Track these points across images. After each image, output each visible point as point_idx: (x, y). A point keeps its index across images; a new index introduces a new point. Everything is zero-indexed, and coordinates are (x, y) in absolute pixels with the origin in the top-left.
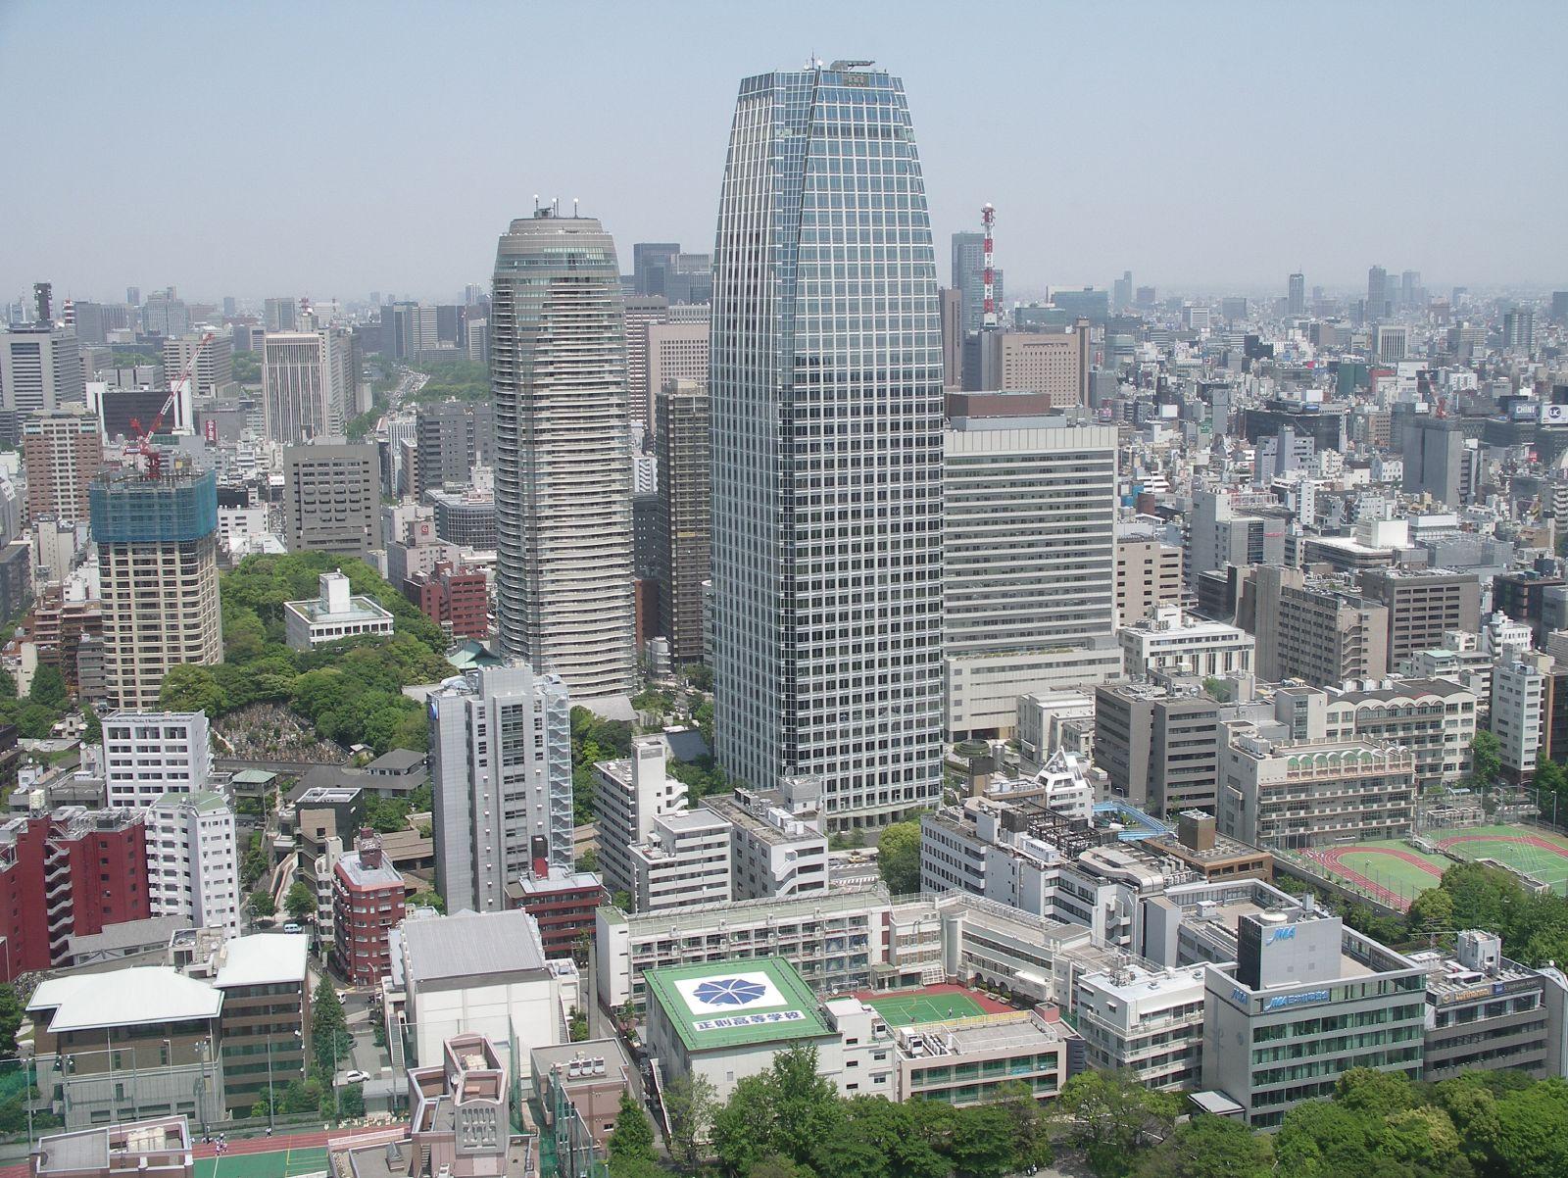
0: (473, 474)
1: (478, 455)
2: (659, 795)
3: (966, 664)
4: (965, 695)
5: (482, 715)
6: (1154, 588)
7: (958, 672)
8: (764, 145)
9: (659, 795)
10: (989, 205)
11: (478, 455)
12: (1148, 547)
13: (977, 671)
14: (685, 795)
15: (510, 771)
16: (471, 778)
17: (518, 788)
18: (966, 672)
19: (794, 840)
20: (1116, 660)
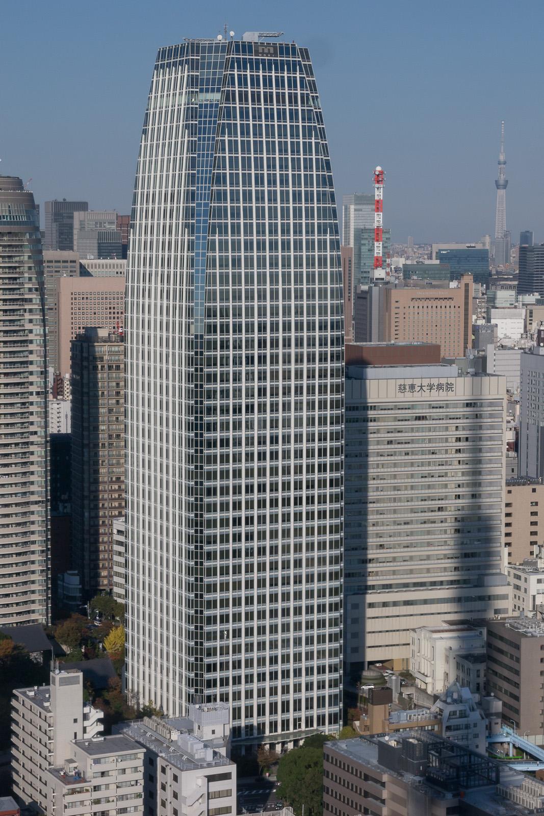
2: (75, 721)
8: (179, 110)
10: (379, 169)
14: (99, 720)
19: (202, 767)
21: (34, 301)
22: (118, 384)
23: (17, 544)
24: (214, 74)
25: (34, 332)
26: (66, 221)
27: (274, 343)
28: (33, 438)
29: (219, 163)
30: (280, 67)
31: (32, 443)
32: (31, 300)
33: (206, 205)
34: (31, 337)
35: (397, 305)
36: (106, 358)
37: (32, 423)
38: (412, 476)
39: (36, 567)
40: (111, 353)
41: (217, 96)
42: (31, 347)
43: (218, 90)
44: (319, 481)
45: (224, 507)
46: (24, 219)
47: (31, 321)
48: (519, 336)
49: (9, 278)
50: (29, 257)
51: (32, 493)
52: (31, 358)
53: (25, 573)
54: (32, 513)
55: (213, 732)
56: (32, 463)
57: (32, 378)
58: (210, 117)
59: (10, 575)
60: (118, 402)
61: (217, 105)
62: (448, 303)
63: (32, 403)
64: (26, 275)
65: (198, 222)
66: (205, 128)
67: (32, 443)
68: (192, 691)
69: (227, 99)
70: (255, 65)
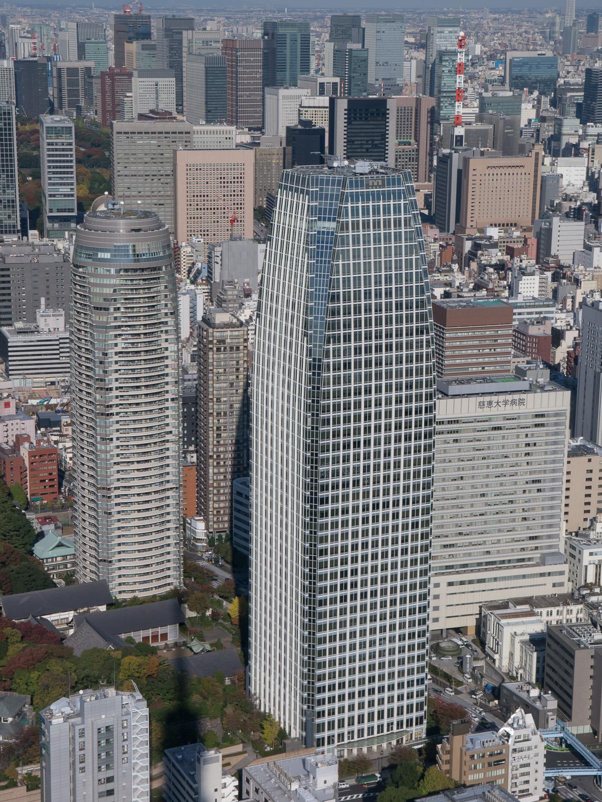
0: (38, 317)
1: (43, 300)
3: (444, 580)
4: (442, 602)
5: (82, 734)
6: (593, 508)
7: (437, 585)
8: (300, 233)
9: (216, 790)
11: (43, 300)
12: (590, 460)
13: (450, 584)
15: (104, 775)
16: (73, 779)
17: (110, 786)
18: (443, 590)
20: (562, 573)
21: (169, 324)
22: (238, 362)
23: (155, 524)
24: (331, 204)
25: (170, 349)
26: (176, 37)
27: (378, 429)
28: (168, 437)
29: (332, 284)
30: (387, 196)
31: (168, 441)
32: (166, 323)
33: (322, 319)
34: (166, 354)
35: (475, 173)
36: (228, 341)
37: (167, 425)
38: (487, 476)
39: (171, 541)
40: (232, 338)
41: (333, 225)
42: (167, 362)
43: (334, 220)
44: (406, 397)
45: (334, 563)
46: (161, 254)
47: (166, 340)
48: (582, 183)
49: (148, 297)
50: (166, 287)
51: (168, 482)
52: (167, 371)
53: (162, 547)
54: (168, 498)
55: (325, 782)
56: (168, 457)
57: (167, 388)
58: (327, 243)
59: (150, 549)
60: (237, 377)
61: (332, 233)
62: (519, 170)
63: (167, 408)
64: (163, 302)
65: (315, 332)
66: (322, 252)
67: (168, 441)
68: (305, 707)
69: (342, 229)
70: (366, 197)
